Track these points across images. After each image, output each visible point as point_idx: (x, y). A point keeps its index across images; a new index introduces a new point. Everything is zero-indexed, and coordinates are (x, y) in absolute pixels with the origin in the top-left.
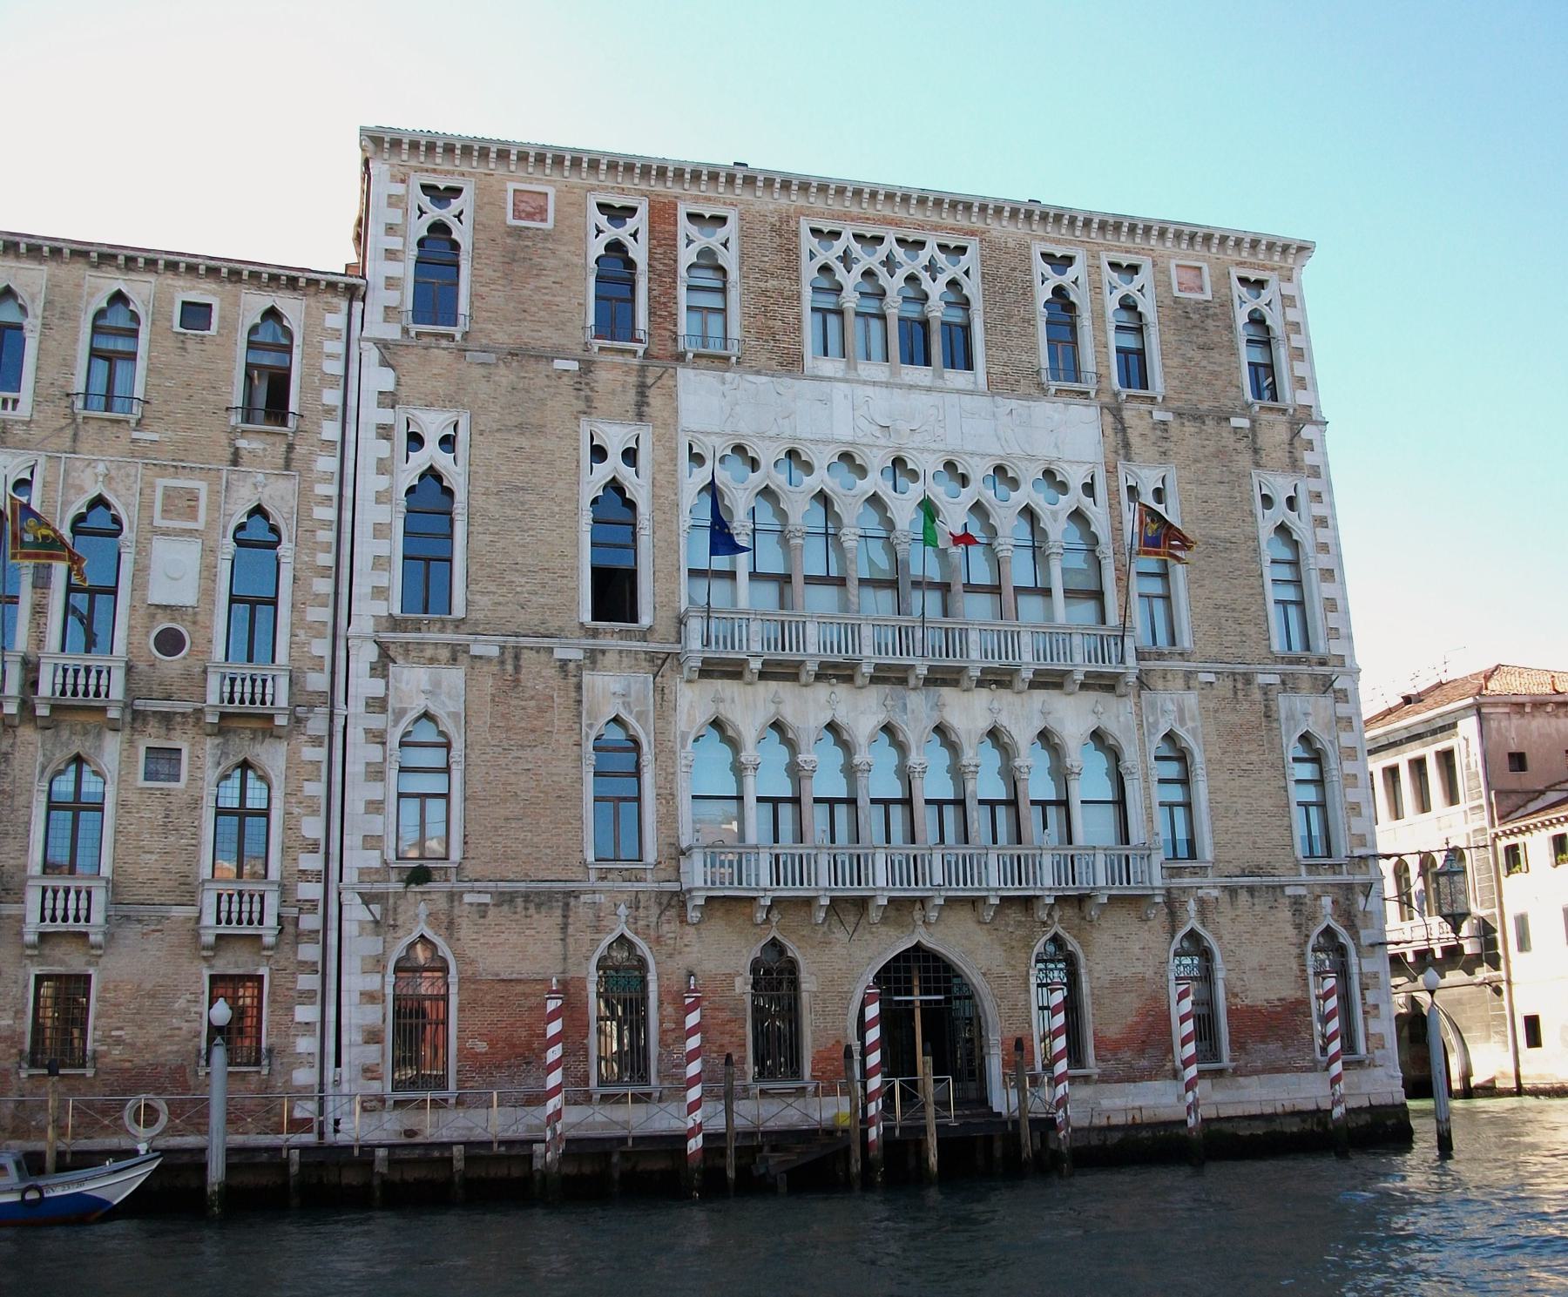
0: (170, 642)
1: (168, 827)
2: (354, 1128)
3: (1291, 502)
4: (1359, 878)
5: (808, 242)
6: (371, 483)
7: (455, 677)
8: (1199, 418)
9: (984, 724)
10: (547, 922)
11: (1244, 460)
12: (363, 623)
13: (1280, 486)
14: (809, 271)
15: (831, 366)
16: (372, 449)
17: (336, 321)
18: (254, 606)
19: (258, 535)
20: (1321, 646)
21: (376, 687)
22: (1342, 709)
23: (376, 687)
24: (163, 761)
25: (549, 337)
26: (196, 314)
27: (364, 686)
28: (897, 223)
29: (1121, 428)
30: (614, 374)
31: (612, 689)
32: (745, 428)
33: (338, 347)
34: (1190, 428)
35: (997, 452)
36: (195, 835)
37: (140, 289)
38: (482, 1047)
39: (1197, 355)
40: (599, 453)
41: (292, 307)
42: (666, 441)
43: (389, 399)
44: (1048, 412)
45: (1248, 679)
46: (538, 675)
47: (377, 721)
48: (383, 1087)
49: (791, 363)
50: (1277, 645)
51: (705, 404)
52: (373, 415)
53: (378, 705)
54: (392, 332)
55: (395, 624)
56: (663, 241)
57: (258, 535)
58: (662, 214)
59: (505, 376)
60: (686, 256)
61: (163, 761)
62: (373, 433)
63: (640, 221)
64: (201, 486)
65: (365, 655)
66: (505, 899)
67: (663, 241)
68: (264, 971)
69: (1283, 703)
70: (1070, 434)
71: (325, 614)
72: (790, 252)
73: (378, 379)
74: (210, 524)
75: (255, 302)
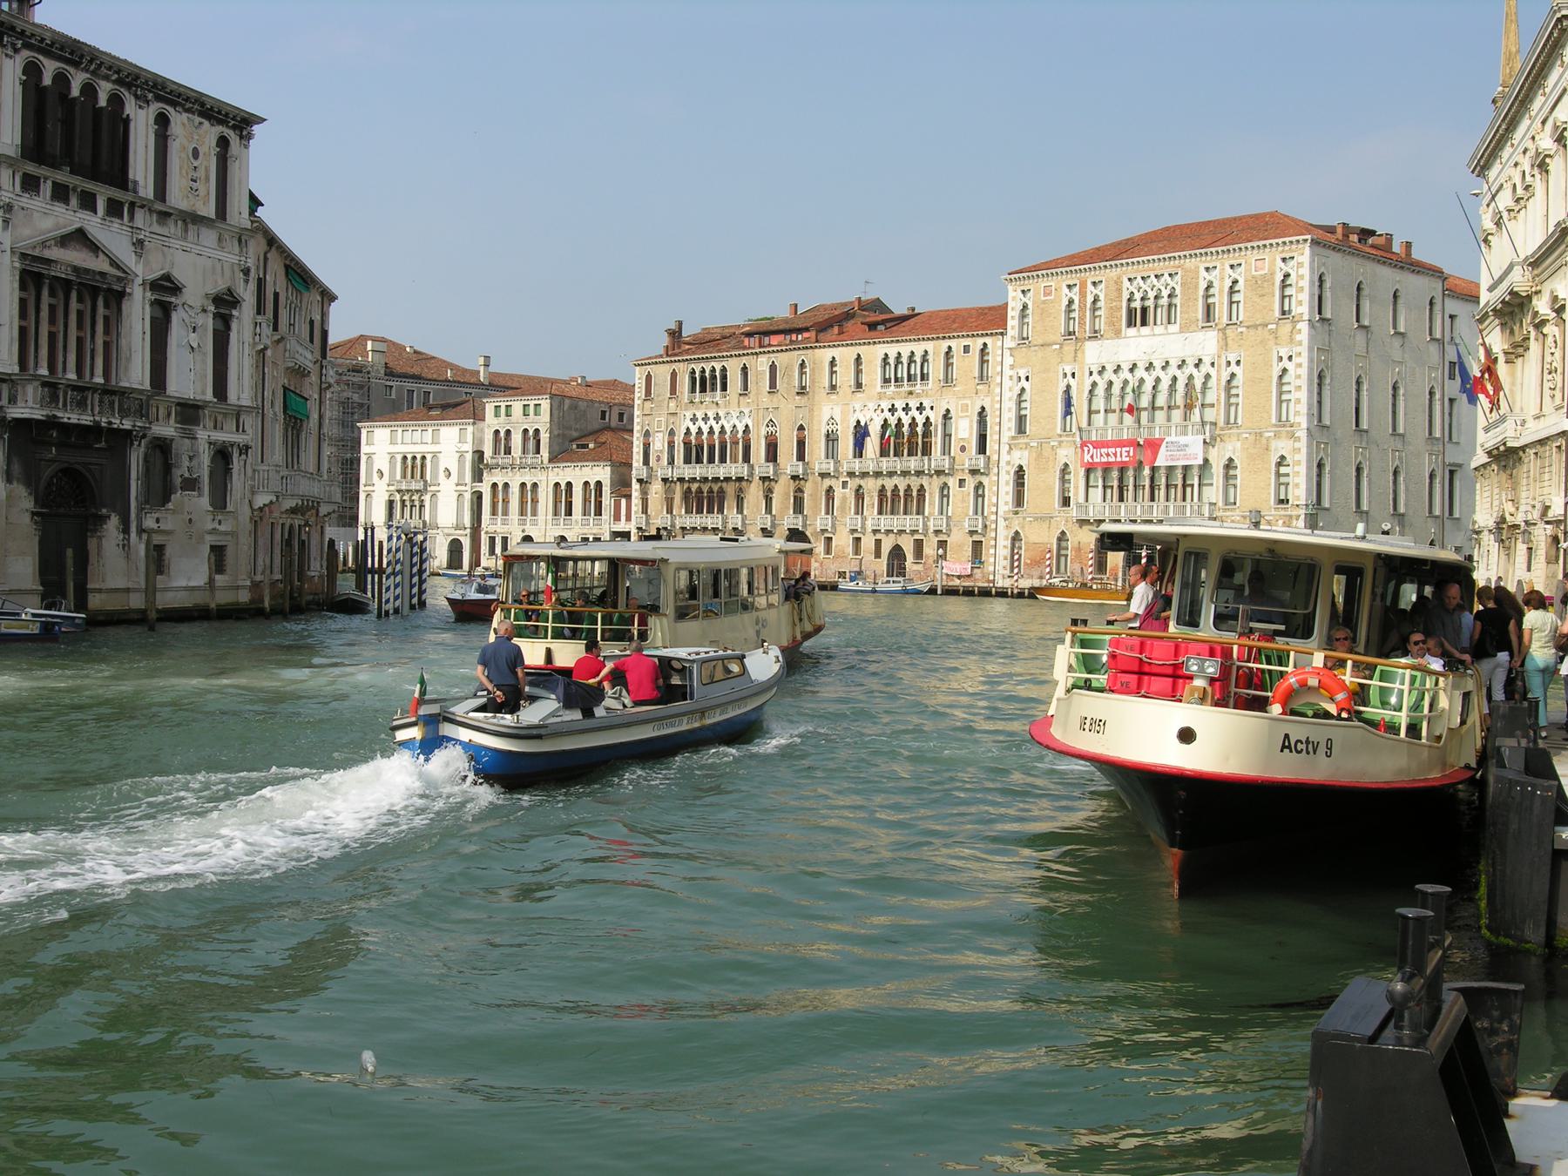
0: (963, 449)
2: (1001, 583)
3: (1290, 358)
4: (1294, 513)
5: (1126, 283)
6: (1007, 395)
7: (1026, 453)
8: (1256, 327)
10: (1045, 525)
11: (1271, 343)
12: (1005, 439)
13: (1284, 353)
14: (1126, 296)
15: (1132, 331)
16: (1007, 383)
19: (982, 413)
20: (1291, 418)
22: (1297, 445)
24: (962, 482)
25: (1051, 338)
27: (1005, 457)
29: (1226, 338)
30: (1069, 348)
31: (1066, 454)
32: (1103, 361)
34: (1252, 332)
35: (1182, 355)
37: (953, 343)
39: (1257, 299)
40: (1065, 375)
41: (988, 340)
42: (1081, 369)
43: (1012, 367)
44: (1201, 335)
45: (1261, 434)
46: (1047, 452)
48: (1007, 572)
49: (1118, 333)
50: (1274, 421)
51: (1094, 353)
52: (1008, 372)
53: (1008, 463)
54: (1013, 345)
55: (1013, 438)
56: (1083, 294)
57: (982, 413)
58: (1083, 286)
59: (1040, 354)
60: (1090, 299)
61: (962, 482)
63: (1077, 289)
65: (1005, 448)
66: (1036, 519)
67: (1083, 294)
69: (1273, 444)
70: (1206, 343)
72: (1120, 290)
73: (1008, 360)
75: (980, 341)
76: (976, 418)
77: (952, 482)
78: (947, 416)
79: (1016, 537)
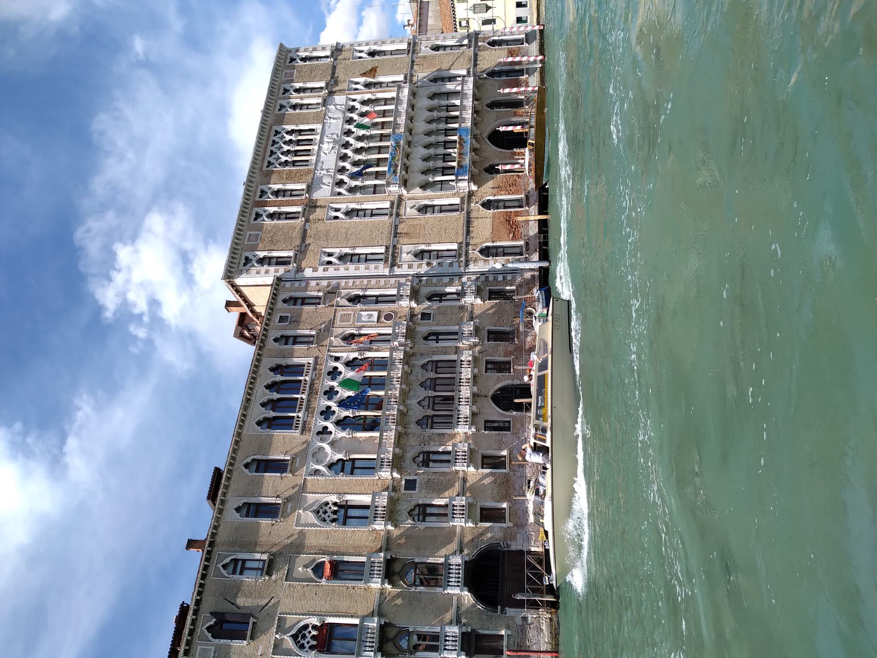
0: (388, 317)
1: (445, 314)
6: (342, 272)
9: (424, 123)
12: (386, 272)
16: (331, 272)
17: (288, 285)
18: (378, 300)
19: (355, 299)
21: (405, 266)
23: (405, 266)
26: (282, 319)
27: (404, 270)
28: (267, 145)
33: (297, 284)
35: (341, 121)
36: (447, 307)
38: (511, 236)
43: (315, 270)
47: (415, 264)
52: (320, 273)
53: (410, 267)
60: (273, 198)
62: (326, 273)
64: (339, 315)
68: (488, 288)
71: (382, 280)
74: (352, 310)
75: (280, 304)
76: (359, 306)
77: (424, 328)
78: (349, 338)
79: (486, 252)
